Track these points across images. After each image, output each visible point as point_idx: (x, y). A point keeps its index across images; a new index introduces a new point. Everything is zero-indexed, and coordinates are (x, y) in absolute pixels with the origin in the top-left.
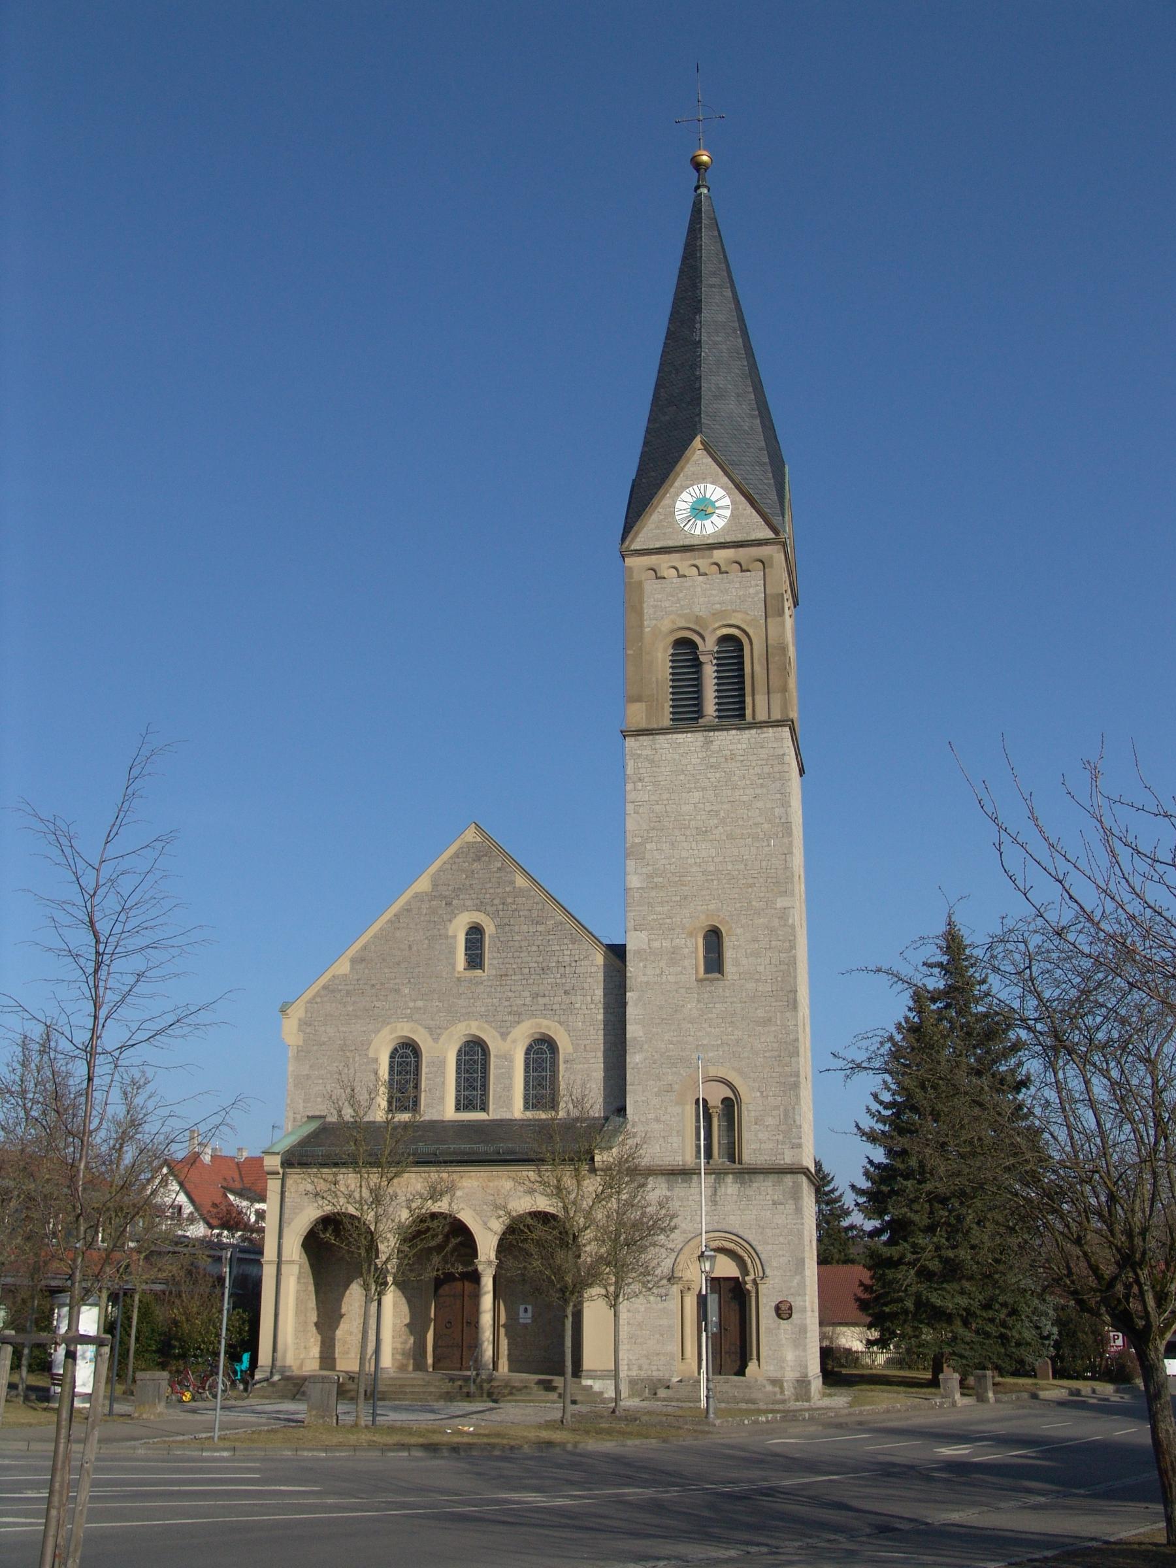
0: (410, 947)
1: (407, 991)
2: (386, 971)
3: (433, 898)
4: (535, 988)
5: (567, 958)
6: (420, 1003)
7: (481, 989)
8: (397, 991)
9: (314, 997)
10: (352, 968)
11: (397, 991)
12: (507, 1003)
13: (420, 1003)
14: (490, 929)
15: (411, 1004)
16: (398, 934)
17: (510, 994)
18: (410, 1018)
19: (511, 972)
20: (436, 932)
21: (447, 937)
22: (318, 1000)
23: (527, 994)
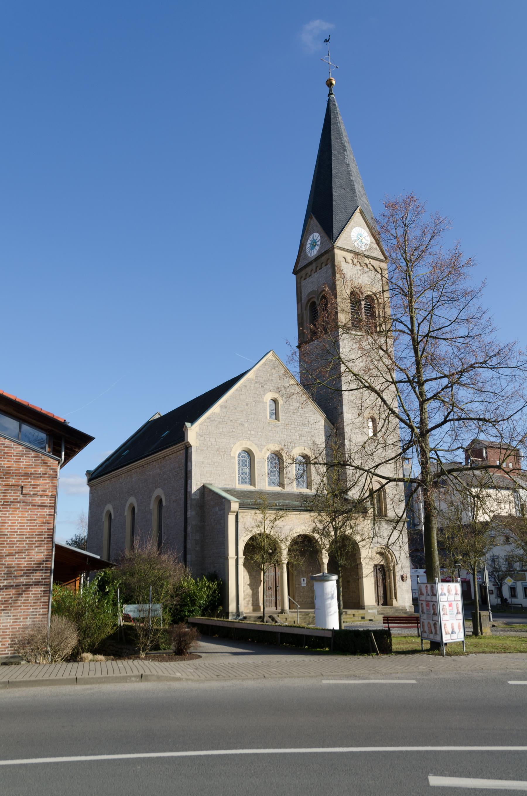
0: (247, 404)
1: (247, 426)
2: (237, 414)
3: (256, 383)
4: (300, 433)
5: (312, 421)
6: (253, 432)
7: (278, 429)
8: (242, 425)
9: (203, 422)
10: (221, 410)
11: (242, 425)
12: (289, 438)
13: (253, 432)
14: (281, 402)
15: (249, 432)
16: (241, 397)
17: (290, 433)
18: (249, 439)
19: (290, 423)
20: (258, 399)
21: (263, 402)
22: (206, 424)
23: (297, 434)
